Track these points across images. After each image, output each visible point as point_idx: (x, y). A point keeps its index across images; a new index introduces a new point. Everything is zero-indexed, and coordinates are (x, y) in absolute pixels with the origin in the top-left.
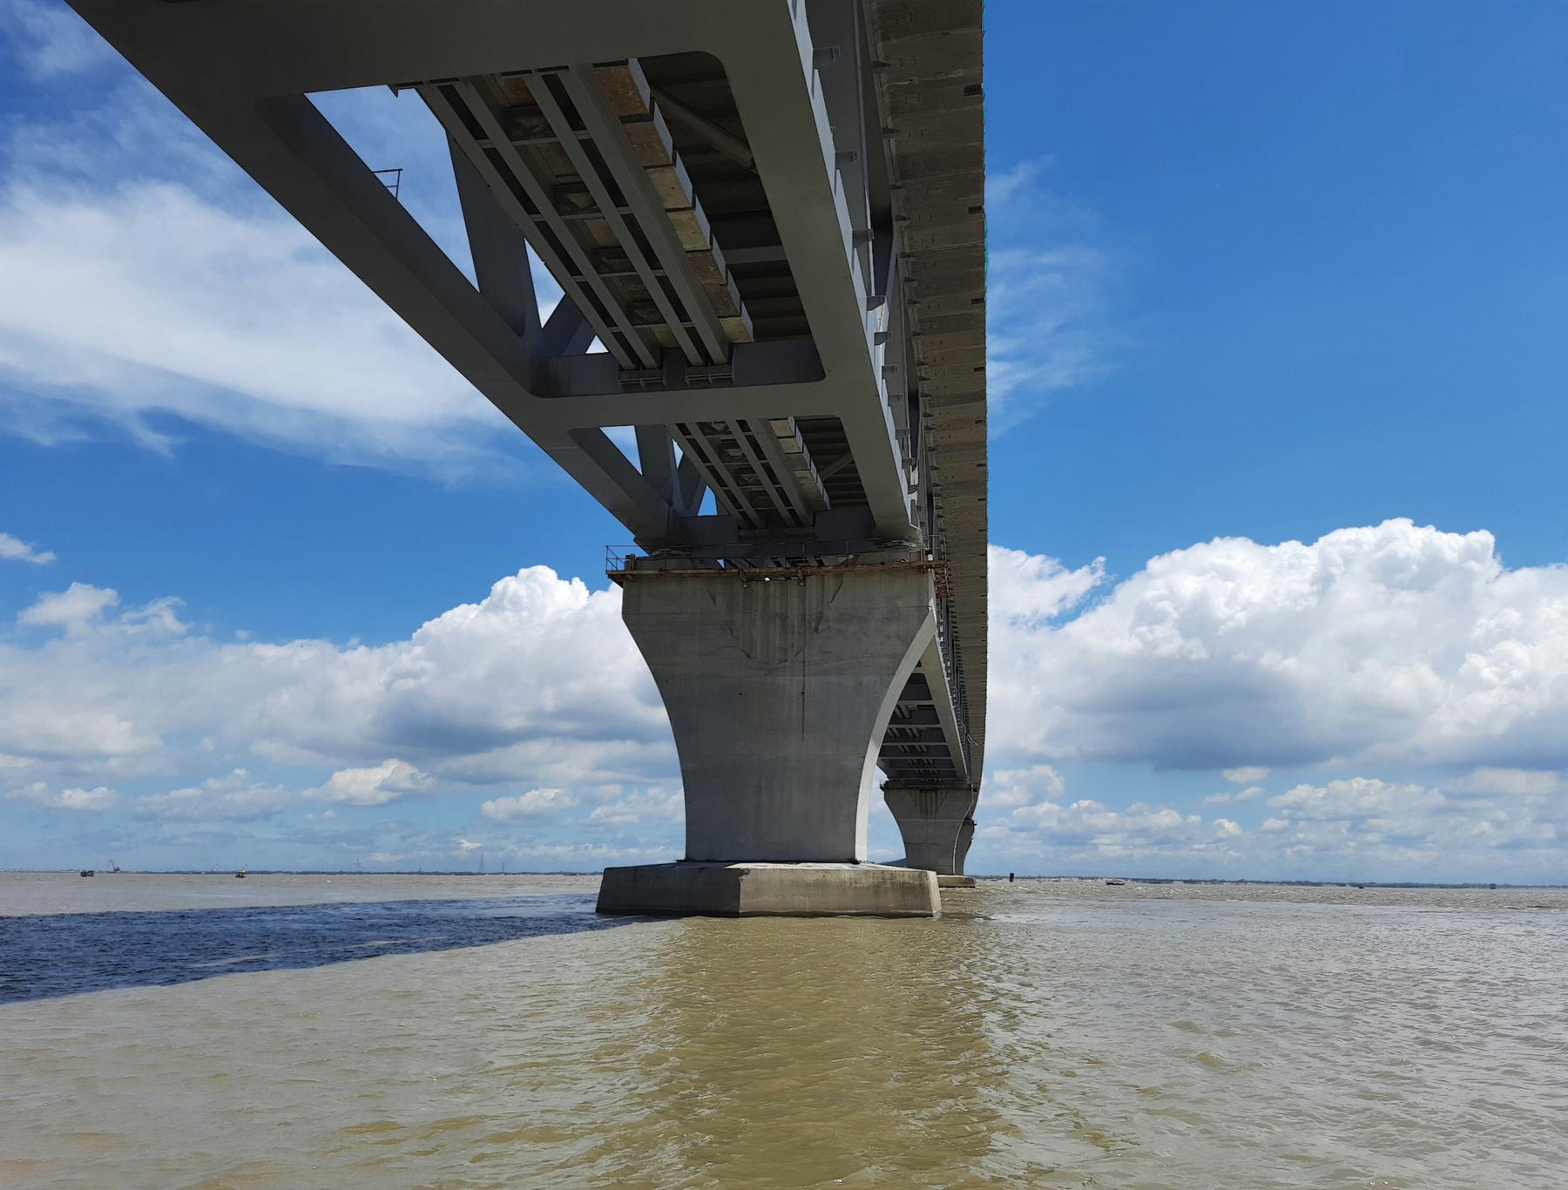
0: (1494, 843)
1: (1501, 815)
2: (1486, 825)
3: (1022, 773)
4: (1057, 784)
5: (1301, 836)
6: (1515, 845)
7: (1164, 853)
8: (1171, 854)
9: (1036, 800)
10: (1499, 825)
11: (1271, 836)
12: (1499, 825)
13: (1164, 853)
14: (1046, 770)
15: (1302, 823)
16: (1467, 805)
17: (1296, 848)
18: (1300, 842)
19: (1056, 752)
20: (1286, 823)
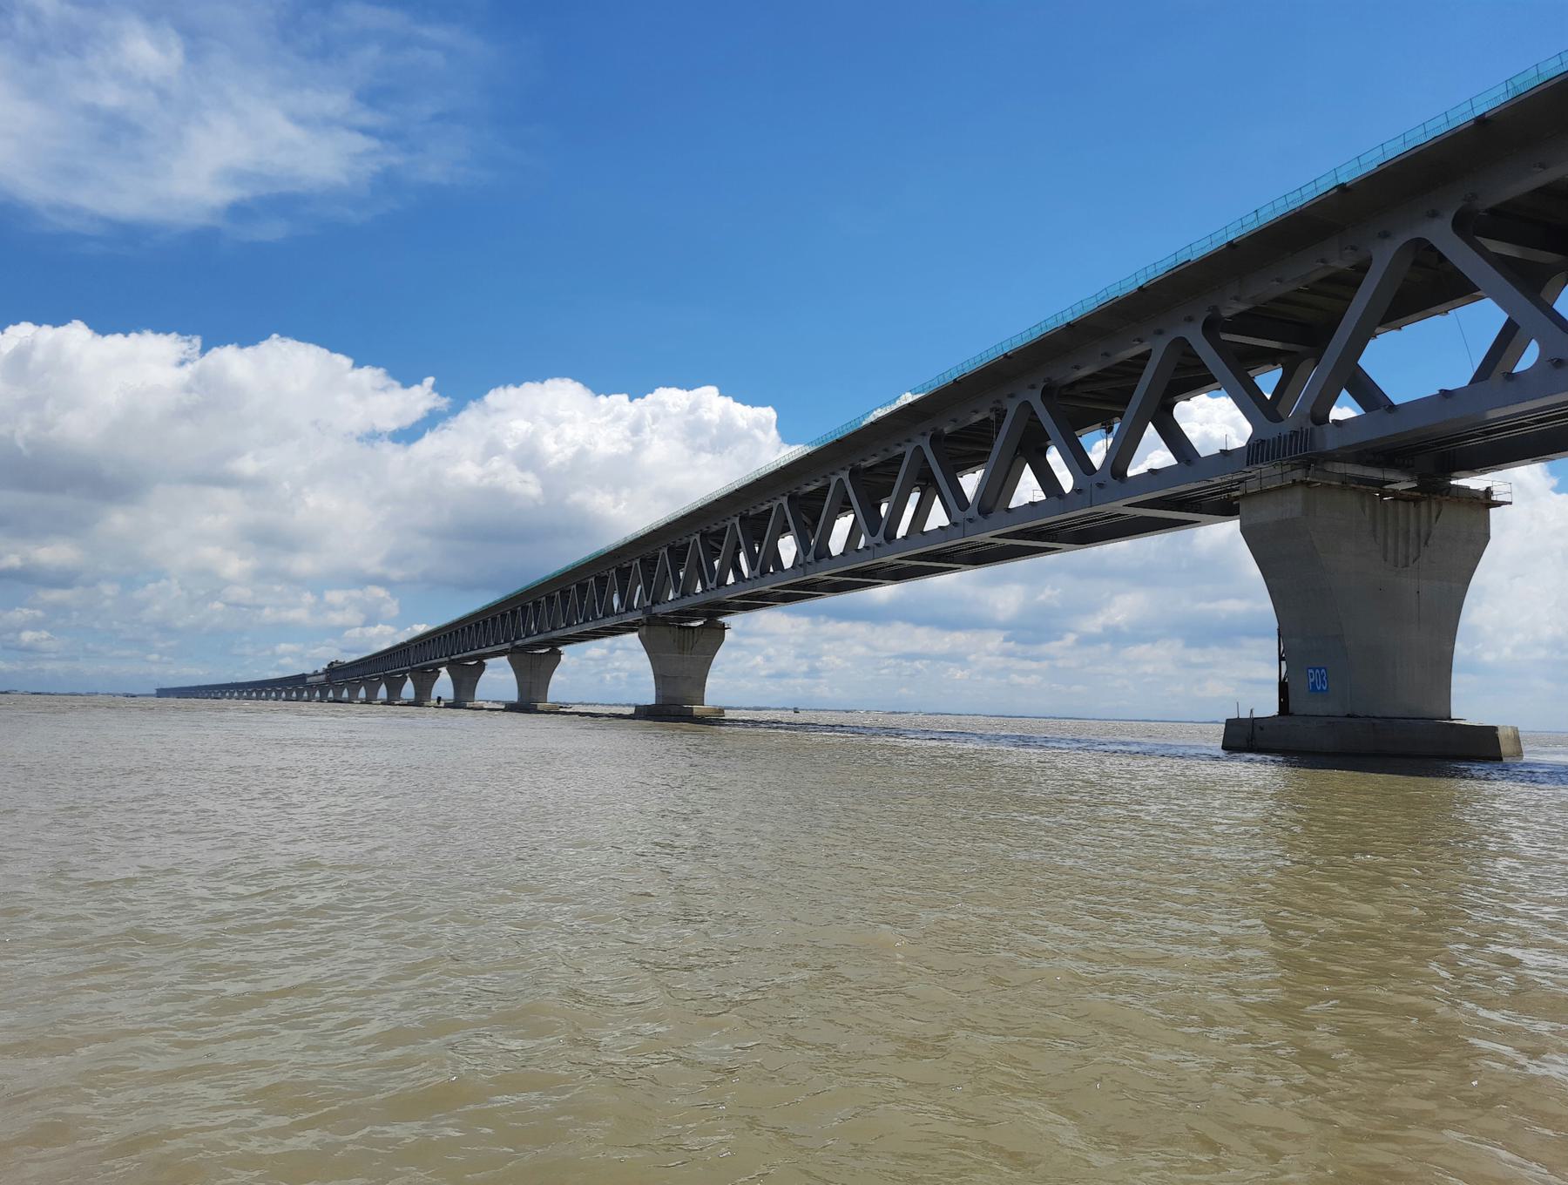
0: (763, 673)
1: (771, 651)
2: (759, 659)
3: (355, 593)
4: (392, 608)
5: (617, 664)
6: (780, 675)
7: (495, 676)
8: (502, 677)
9: (370, 621)
10: (768, 659)
11: (591, 663)
12: (768, 659)
13: (495, 676)
14: (381, 593)
15: (618, 652)
16: (746, 641)
17: (615, 674)
18: (617, 669)
19: (396, 574)
20: (605, 651)
